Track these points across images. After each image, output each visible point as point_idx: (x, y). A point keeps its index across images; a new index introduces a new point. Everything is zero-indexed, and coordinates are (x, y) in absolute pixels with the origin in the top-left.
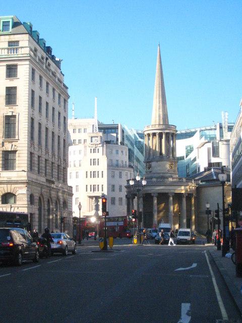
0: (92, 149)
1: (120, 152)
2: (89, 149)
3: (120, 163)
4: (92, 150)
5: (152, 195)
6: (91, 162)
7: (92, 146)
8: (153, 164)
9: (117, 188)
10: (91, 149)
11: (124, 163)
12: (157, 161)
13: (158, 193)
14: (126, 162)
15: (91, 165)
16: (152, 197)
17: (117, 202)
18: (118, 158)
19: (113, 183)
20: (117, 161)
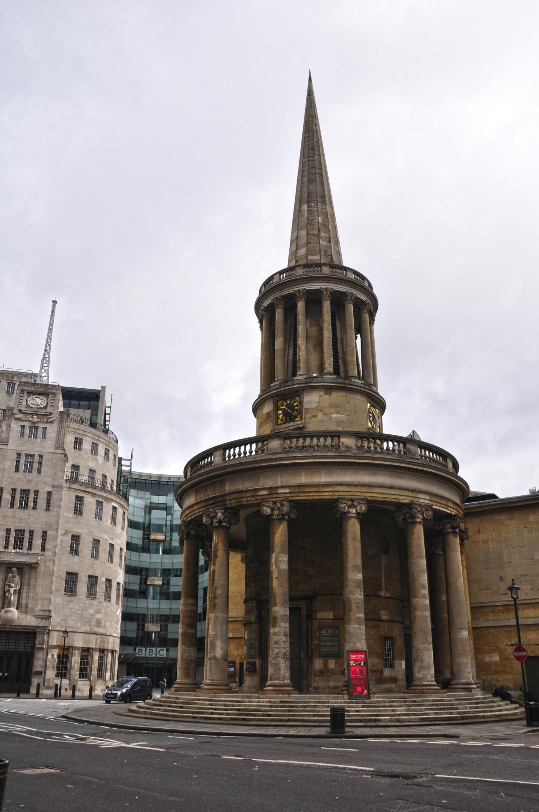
0: (27, 424)
1: (101, 450)
2: (15, 427)
3: (98, 477)
4: (27, 430)
5: (343, 506)
6: (18, 462)
7: (29, 418)
8: (311, 400)
9: (86, 547)
10: (23, 427)
11: (109, 481)
12: (328, 389)
13: (370, 503)
14: (112, 481)
15: (17, 470)
16: (344, 517)
17: (82, 587)
18: (92, 465)
19: (76, 530)
20: (92, 471)
